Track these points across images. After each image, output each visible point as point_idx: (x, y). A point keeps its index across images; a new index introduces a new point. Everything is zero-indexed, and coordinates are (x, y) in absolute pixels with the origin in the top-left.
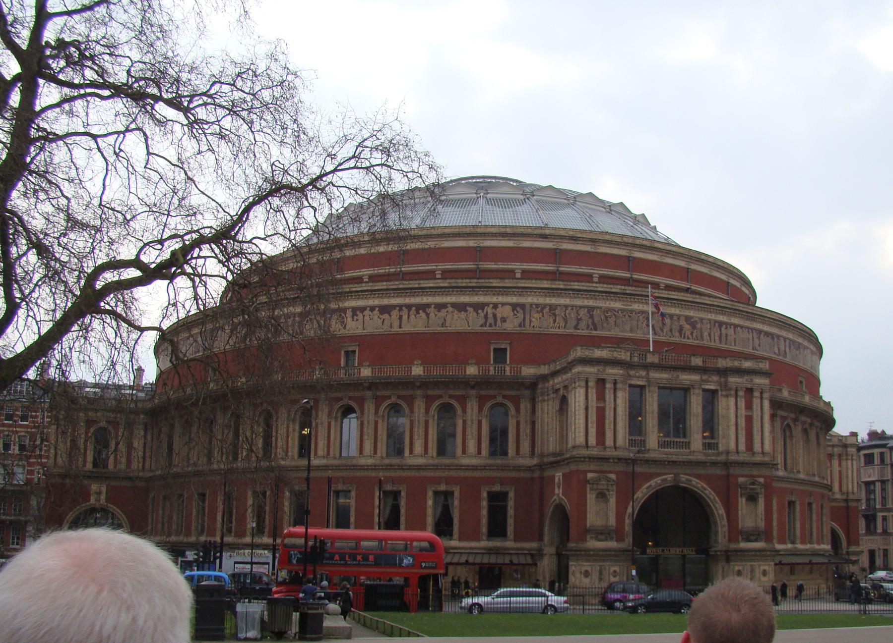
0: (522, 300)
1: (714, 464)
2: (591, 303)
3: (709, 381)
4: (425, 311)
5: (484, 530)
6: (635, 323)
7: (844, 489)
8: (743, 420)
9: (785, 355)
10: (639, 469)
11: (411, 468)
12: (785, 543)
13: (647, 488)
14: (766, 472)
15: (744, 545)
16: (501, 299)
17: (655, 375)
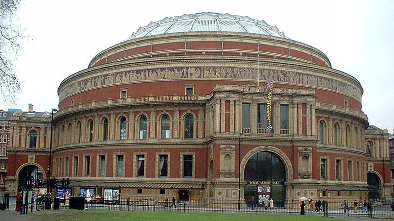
0: (200, 65)
1: (285, 141)
2: (233, 65)
3: (284, 100)
4: (155, 72)
5: (182, 172)
6: (255, 74)
7: (382, 156)
8: (301, 119)
10: (243, 143)
11: (149, 144)
12: (334, 180)
13: (251, 152)
14: (313, 144)
15: (300, 180)
16: (190, 65)
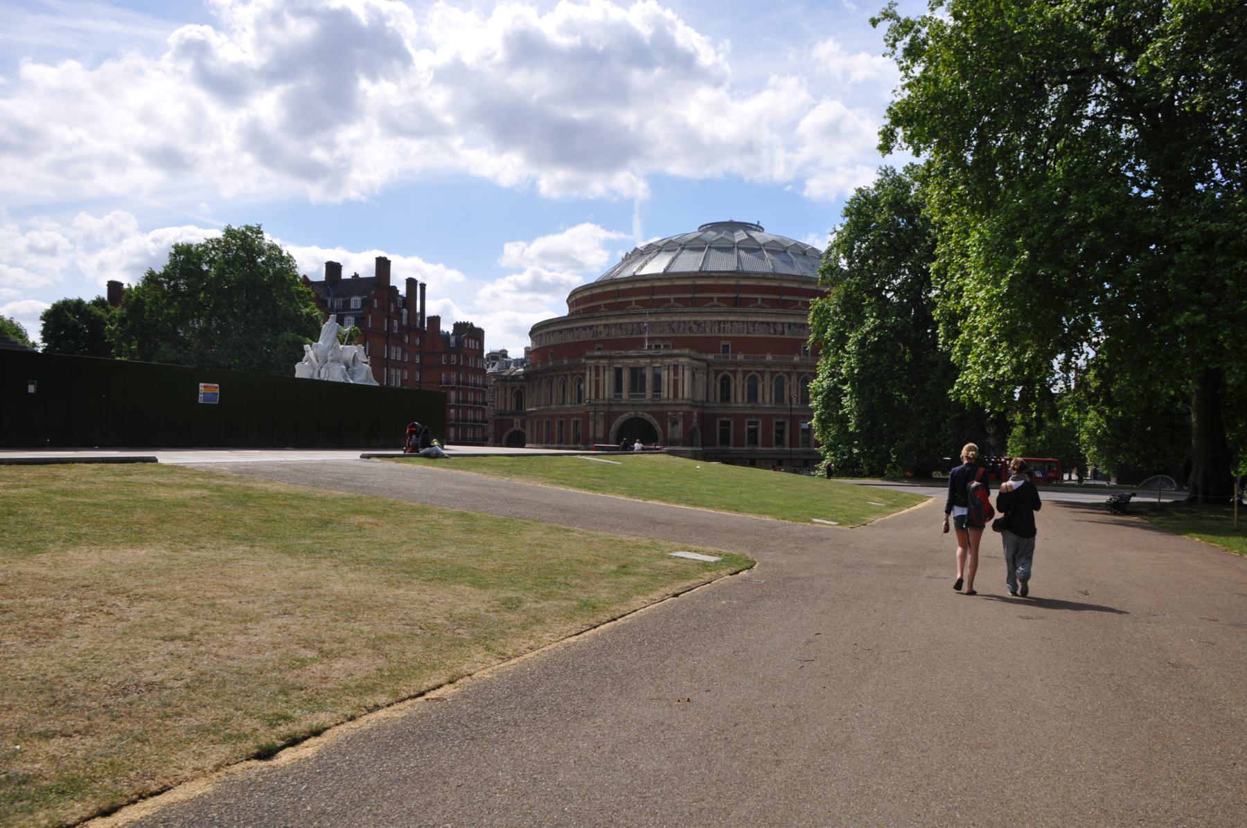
2: (639, 320)
9: (783, 332)
17: (627, 361)
